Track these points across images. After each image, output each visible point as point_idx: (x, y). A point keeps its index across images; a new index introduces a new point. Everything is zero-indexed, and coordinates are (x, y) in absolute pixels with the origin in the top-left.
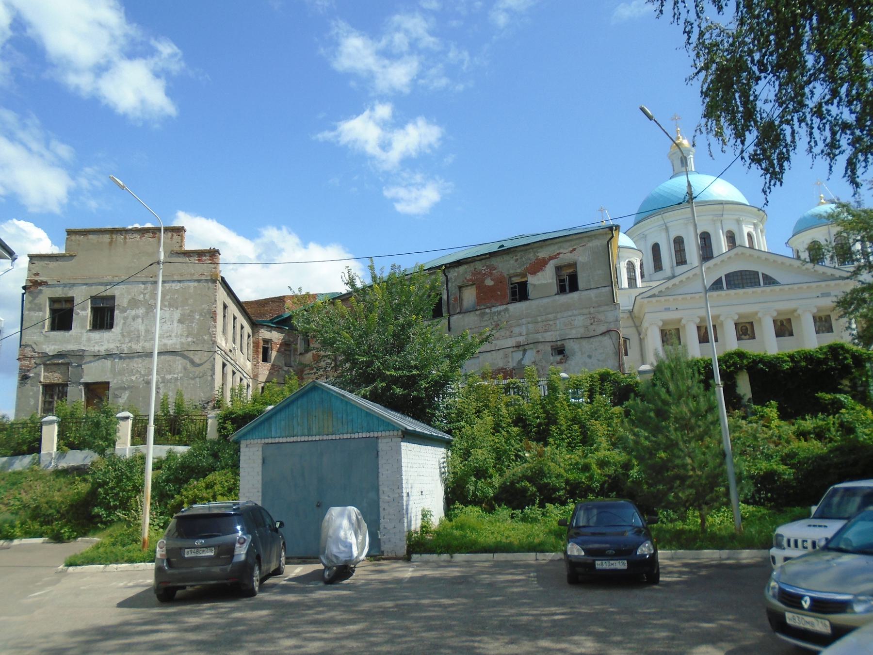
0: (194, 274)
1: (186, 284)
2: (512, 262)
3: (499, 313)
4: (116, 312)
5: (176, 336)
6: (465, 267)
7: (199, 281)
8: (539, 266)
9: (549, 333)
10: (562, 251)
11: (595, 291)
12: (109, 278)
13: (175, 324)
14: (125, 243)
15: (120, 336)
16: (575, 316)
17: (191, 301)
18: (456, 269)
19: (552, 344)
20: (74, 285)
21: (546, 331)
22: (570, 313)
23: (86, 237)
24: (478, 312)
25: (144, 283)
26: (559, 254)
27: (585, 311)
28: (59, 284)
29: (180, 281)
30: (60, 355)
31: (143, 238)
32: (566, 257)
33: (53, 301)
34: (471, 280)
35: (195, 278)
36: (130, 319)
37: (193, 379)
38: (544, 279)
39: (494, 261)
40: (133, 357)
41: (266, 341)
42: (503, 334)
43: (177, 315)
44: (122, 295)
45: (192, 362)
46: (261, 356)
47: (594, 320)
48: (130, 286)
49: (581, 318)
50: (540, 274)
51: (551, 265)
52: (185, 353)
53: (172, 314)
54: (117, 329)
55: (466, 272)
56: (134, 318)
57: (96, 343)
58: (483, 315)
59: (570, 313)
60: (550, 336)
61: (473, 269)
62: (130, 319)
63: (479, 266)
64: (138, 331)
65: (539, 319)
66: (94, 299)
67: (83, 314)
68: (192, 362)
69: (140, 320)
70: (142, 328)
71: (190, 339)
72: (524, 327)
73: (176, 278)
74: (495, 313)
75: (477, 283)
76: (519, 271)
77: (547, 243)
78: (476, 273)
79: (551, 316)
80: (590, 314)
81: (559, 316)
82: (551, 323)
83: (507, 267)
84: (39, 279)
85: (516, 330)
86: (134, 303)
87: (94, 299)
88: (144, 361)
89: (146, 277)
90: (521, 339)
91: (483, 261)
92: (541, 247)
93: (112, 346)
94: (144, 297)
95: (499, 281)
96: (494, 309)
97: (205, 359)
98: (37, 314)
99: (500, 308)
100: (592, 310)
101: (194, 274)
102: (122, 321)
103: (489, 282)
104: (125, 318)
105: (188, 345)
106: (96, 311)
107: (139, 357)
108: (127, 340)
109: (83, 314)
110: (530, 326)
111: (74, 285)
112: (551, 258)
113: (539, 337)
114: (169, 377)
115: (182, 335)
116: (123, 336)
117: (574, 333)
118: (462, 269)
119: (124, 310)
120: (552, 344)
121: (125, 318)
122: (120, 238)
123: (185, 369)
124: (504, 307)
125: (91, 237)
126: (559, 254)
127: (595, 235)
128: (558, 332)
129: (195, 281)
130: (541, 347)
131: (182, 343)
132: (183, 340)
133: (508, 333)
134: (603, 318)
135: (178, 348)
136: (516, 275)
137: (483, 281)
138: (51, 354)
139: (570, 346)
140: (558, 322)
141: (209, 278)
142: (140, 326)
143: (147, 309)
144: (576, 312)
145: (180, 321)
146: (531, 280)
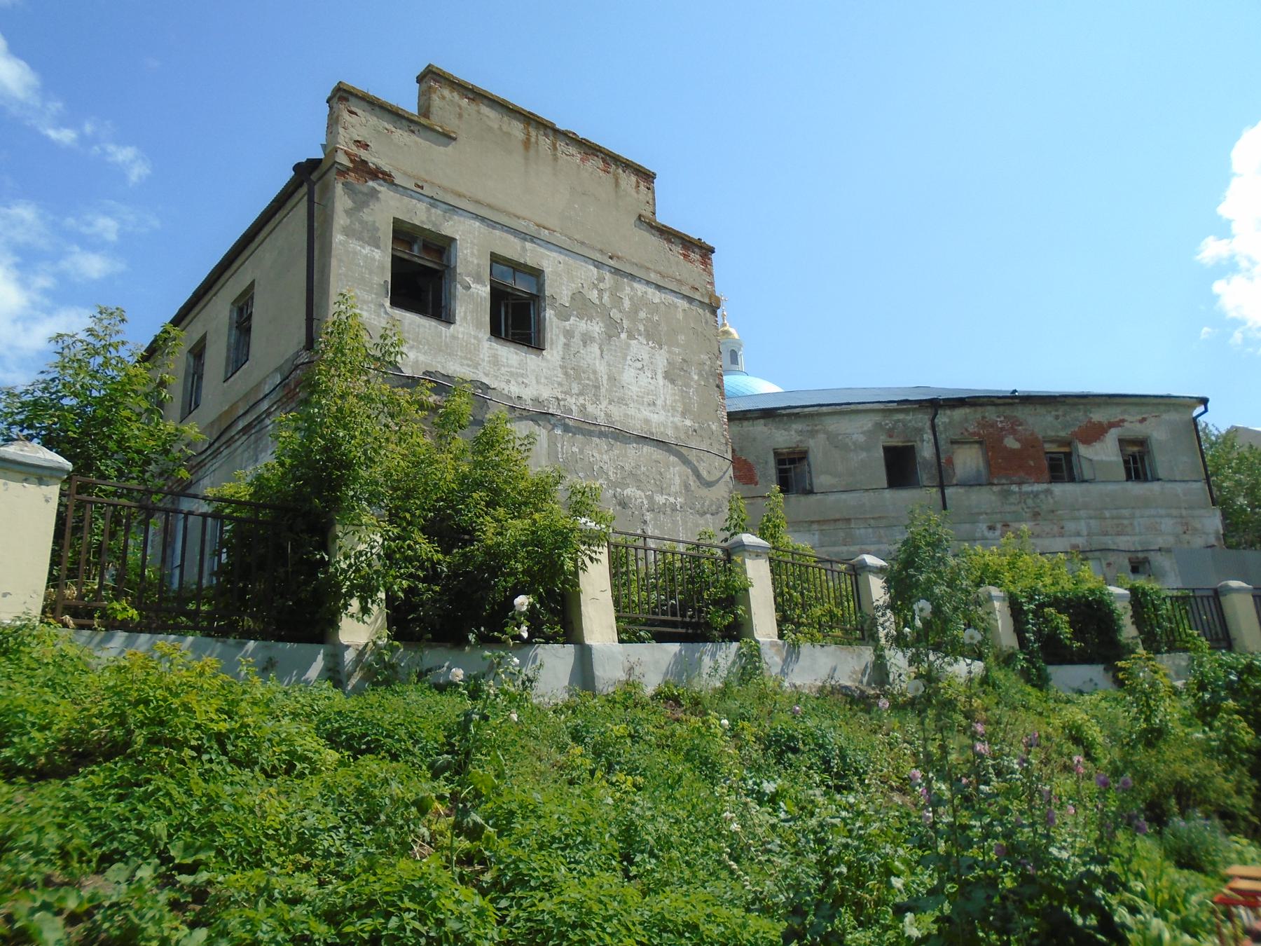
1: (670, 298)
2: (1050, 418)
3: (1036, 495)
6: (967, 410)
7: (690, 300)
8: (1094, 433)
9: (1125, 538)
10: (1126, 417)
11: (1183, 485)
12: (532, 229)
13: (661, 381)
15: (559, 373)
16: (1161, 517)
17: (681, 338)
18: (948, 412)
19: (1129, 555)
20: (454, 209)
21: (1118, 534)
22: (1153, 512)
23: (473, 107)
24: (995, 489)
25: (598, 265)
26: (1123, 421)
27: (1175, 512)
28: (417, 191)
29: (659, 287)
31: (588, 164)
32: (1134, 428)
33: (404, 234)
34: (974, 434)
35: (686, 290)
36: (577, 340)
38: (1104, 453)
39: (1021, 413)
40: (590, 434)
42: (1047, 529)
44: (563, 278)
45: (698, 475)
47: (1187, 528)
48: (571, 261)
49: (1170, 522)
50: (1097, 445)
51: (1113, 434)
52: (683, 450)
54: (553, 353)
55: (966, 420)
56: (587, 339)
57: (512, 374)
58: (1006, 494)
59: (1153, 512)
60: (1124, 542)
61: (979, 416)
62: (577, 340)
63: (991, 413)
64: (595, 372)
65: (1107, 514)
66: (495, 259)
67: (472, 296)
68: (698, 475)
69: (595, 348)
70: (601, 368)
71: (688, 423)
72: (1083, 523)
73: (653, 277)
74: (1028, 493)
75: (989, 442)
76: (1063, 434)
77: (1115, 400)
78: (984, 424)
79: (1126, 512)
80: (1181, 517)
81: (1138, 513)
82: (1126, 522)
83: (1043, 424)
85: (1071, 526)
87: (495, 259)
88: (611, 447)
89: (601, 251)
90: (1080, 541)
91: (1001, 409)
92: (1099, 405)
93: (545, 393)
94: (601, 298)
95: (1031, 444)
96: (1026, 488)
97: (719, 474)
98: (367, 250)
99: (1037, 487)
100: (1184, 512)
102: (562, 340)
103: (1011, 443)
107: (602, 435)
109: (472, 296)
110: (1093, 522)
111: (454, 209)
112: (1112, 425)
113: (1109, 541)
114: (660, 499)
117: (1160, 542)
118: (959, 413)
120: (1133, 555)
121: (569, 334)
122: (545, 142)
123: (687, 487)
124: (1045, 486)
125: (485, 110)
126: (1123, 421)
127: (1174, 404)
128: (1137, 538)
129: (685, 297)
130: (1112, 558)
131: (676, 428)
133: (1056, 529)
134: (1199, 526)
135: (670, 435)
136: (1052, 441)
137: (1001, 440)
139: (1158, 560)
140: (1136, 523)
141: (707, 301)
143: (607, 326)
144: (1162, 512)
146: (1083, 450)
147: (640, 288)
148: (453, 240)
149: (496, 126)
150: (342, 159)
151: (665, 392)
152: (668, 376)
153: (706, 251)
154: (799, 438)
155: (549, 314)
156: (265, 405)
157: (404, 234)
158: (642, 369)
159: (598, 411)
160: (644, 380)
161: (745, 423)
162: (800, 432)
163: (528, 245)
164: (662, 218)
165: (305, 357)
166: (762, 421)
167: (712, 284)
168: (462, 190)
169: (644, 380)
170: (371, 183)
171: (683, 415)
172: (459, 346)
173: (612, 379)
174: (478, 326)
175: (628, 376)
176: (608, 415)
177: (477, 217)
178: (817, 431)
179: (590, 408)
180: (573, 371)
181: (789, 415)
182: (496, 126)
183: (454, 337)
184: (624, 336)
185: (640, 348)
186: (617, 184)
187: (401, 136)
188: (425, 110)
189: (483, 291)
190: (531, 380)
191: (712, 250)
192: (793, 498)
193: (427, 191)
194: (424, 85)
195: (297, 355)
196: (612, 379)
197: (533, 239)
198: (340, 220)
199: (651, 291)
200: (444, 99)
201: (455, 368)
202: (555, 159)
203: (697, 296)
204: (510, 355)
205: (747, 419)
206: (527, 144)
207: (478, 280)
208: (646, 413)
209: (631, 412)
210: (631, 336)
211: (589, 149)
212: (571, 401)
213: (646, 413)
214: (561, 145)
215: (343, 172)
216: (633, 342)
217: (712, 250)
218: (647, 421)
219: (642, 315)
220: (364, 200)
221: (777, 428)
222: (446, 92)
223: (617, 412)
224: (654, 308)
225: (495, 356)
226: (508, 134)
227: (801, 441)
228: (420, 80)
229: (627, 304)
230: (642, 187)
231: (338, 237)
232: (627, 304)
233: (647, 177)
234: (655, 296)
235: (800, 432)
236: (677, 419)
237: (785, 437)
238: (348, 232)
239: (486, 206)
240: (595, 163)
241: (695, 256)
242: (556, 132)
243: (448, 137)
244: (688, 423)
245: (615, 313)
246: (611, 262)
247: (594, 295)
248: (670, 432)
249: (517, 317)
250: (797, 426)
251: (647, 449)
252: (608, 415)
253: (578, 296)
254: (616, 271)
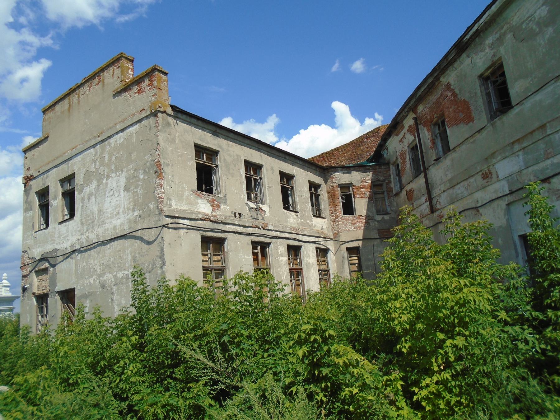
0: (134, 115)
4: (76, 193)
5: (124, 212)
13: (122, 193)
14: (79, 101)
41: (345, 187)
46: (340, 208)
52: (134, 234)
101: (134, 115)
104: (83, 199)
105: (136, 222)
115: (128, 209)
116: (82, 224)
125: (57, 108)
132: (130, 216)
141: (149, 113)
145: (127, 189)
154: (492, 52)
161: (456, 65)
166: (464, 55)
178: (505, 34)
205: (454, 60)
221: (476, 54)
227: (494, 55)
235: (492, 46)
237: (477, 61)
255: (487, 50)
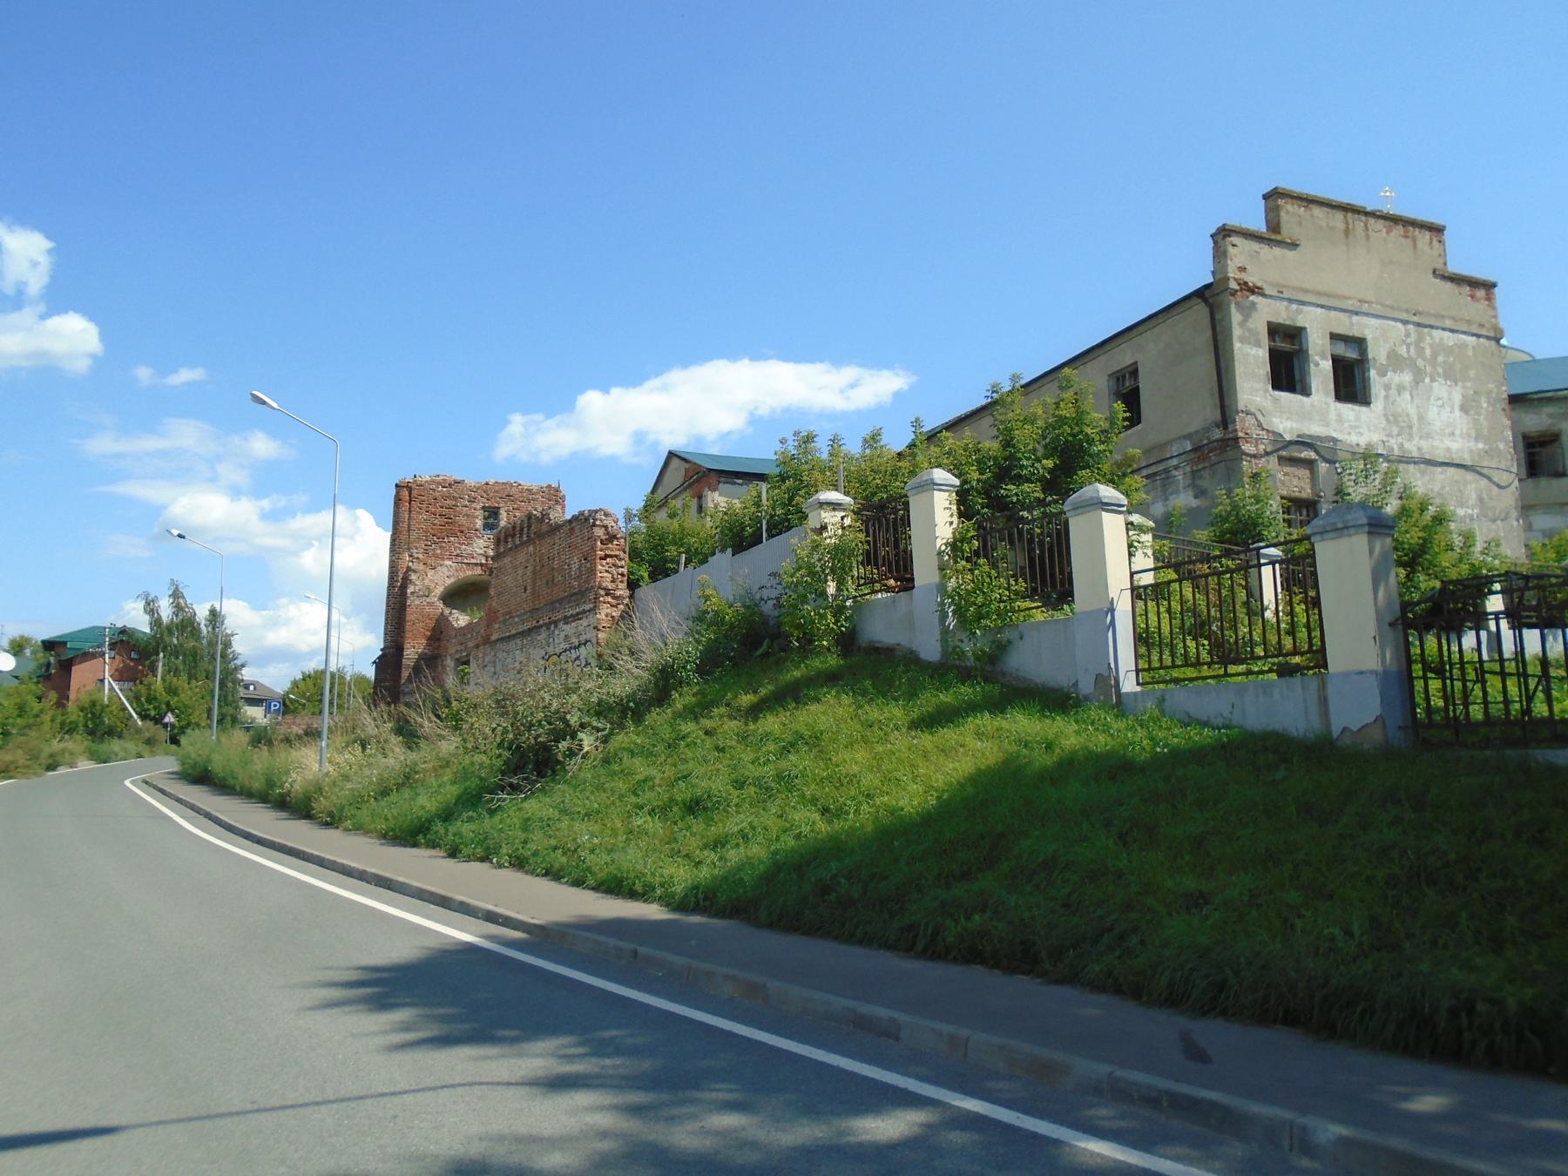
13: (1457, 413)
17: (1472, 373)
25: (1405, 322)
29: (1452, 331)
30: (1303, 443)
33: (1274, 330)
36: (1393, 392)
37: (1494, 521)
43: (1457, 398)
53: (1450, 394)
54: (1378, 405)
56: (1401, 388)
57: (1352, 427)
62: (1393, 392)
67: (1321, 371)
70: (1412, 411)
71: (1480, 446)
73: (1448, 323)
84: (1251, 279)
86: (1396, 362)
87: (1334, 337)
88: (1423, 473)
89: (1407, 311)
102: (1383, 393)
106: (1337, 362)
108: (1395, 430)
109: (1321, 371)
119: (1383, 374)
121: (1387, 387)
122: (1358, 223)
131: (1471, 451)
138: (1288, 437)
142: (1406, 403)
143: (1415, 375)
147: (1437, 334)
148: (1304, 329)
149: (1323, 224)
150: (1233, 285)
151: (1461, 422)
152: (1464, 409)
153: (1489, 286)
155: (1373, 373)
156: (1175, 462)
157: (1274, 330)
158: (1442, 406)
159: (1412, 447)
160: (1445, 414)
162: (1551, 416)
163: (1355, 319)
164: (1454, 267)
165: (1218, 434)
167: (1495, 317)
168: (1306, 285)
169: (1445, 414)
170: (1252, 298)
171: (1476, 439)
172: (1316, 413)
173: (1421, 418)
174: (1327, 394)
175: (1432, 413)
176: (1419, 449)
177: (1318, 306)
179: (1407, 445)
180: (1392, 418)
181: (1540, 400)
182: (1323, 224)
183: (1312, 406)
184: (1427, 380)
185: (1440, 388)
186: (1415, 246)
187: (1265, 251)
188: (1274, 226)
189: (1327, 365)
190: (1364, 430)
191: (1494, 285)
192: (1543, 482)
193: (1286, 295)
194: (1271, 204)
195: (1207, 429)
196: (1421, 418)
197: (1357, 313)
198: (1237, 332)
199: (1447, 334)
200: (1289, 211)
201: (1315, 429)
202: (1368, 237)
203: (1484, 332)
204: (1349, 410)
206: (1347, 232)
207: (1323, 357)
208: (1448, 443)
209: (1436, 443)
210: (1433, 380)
211: (1394, 220)
212: (1393, 442)
213: (1448, 443)
214: (1372, 221)
215: (1234, 293)
216: (1435, 384)
217: (1494, 285)
218: (1448, 449)
219: (1440, 359)
220: (1249, 311)
222: (1289, 207)
223: (1425, 445)
224: (1449, 351)
225: (1339, 415)
226: (1333, 228)
228: (1265, 197)
229: (1428, 352)
230: (1435, 243)
231: (1237, 345)
232: (1428, 352)
233: (1437, 230)
234: (1450, 339)
235: (1551, 416)
236: (1472, 444)
238: (1242, 340)
239: (1314, 287)
240: (1399, 230)
241: (1481, 293)
242: (1367, 214)
243: (1294, 245)
244: (1480, 446)
245: (1420, 363)
246: (1415, 319)
247: (1403, 350)
248: (1466, 456)
249: (1351, 382)
250: (1549, 409)
251: (1451, 470)
252: (1419, 449)
253: (1393, 356)
254: (1419, 325)
255: (1544, 417)
